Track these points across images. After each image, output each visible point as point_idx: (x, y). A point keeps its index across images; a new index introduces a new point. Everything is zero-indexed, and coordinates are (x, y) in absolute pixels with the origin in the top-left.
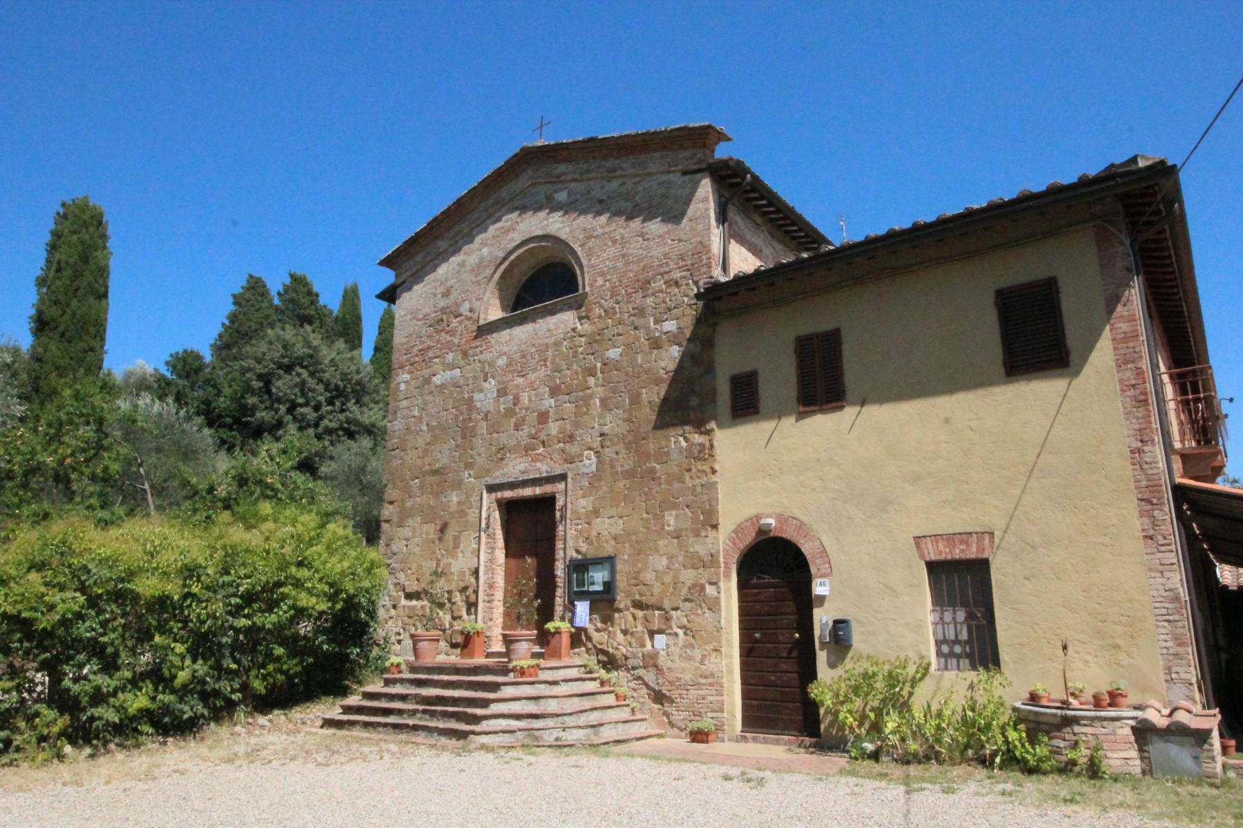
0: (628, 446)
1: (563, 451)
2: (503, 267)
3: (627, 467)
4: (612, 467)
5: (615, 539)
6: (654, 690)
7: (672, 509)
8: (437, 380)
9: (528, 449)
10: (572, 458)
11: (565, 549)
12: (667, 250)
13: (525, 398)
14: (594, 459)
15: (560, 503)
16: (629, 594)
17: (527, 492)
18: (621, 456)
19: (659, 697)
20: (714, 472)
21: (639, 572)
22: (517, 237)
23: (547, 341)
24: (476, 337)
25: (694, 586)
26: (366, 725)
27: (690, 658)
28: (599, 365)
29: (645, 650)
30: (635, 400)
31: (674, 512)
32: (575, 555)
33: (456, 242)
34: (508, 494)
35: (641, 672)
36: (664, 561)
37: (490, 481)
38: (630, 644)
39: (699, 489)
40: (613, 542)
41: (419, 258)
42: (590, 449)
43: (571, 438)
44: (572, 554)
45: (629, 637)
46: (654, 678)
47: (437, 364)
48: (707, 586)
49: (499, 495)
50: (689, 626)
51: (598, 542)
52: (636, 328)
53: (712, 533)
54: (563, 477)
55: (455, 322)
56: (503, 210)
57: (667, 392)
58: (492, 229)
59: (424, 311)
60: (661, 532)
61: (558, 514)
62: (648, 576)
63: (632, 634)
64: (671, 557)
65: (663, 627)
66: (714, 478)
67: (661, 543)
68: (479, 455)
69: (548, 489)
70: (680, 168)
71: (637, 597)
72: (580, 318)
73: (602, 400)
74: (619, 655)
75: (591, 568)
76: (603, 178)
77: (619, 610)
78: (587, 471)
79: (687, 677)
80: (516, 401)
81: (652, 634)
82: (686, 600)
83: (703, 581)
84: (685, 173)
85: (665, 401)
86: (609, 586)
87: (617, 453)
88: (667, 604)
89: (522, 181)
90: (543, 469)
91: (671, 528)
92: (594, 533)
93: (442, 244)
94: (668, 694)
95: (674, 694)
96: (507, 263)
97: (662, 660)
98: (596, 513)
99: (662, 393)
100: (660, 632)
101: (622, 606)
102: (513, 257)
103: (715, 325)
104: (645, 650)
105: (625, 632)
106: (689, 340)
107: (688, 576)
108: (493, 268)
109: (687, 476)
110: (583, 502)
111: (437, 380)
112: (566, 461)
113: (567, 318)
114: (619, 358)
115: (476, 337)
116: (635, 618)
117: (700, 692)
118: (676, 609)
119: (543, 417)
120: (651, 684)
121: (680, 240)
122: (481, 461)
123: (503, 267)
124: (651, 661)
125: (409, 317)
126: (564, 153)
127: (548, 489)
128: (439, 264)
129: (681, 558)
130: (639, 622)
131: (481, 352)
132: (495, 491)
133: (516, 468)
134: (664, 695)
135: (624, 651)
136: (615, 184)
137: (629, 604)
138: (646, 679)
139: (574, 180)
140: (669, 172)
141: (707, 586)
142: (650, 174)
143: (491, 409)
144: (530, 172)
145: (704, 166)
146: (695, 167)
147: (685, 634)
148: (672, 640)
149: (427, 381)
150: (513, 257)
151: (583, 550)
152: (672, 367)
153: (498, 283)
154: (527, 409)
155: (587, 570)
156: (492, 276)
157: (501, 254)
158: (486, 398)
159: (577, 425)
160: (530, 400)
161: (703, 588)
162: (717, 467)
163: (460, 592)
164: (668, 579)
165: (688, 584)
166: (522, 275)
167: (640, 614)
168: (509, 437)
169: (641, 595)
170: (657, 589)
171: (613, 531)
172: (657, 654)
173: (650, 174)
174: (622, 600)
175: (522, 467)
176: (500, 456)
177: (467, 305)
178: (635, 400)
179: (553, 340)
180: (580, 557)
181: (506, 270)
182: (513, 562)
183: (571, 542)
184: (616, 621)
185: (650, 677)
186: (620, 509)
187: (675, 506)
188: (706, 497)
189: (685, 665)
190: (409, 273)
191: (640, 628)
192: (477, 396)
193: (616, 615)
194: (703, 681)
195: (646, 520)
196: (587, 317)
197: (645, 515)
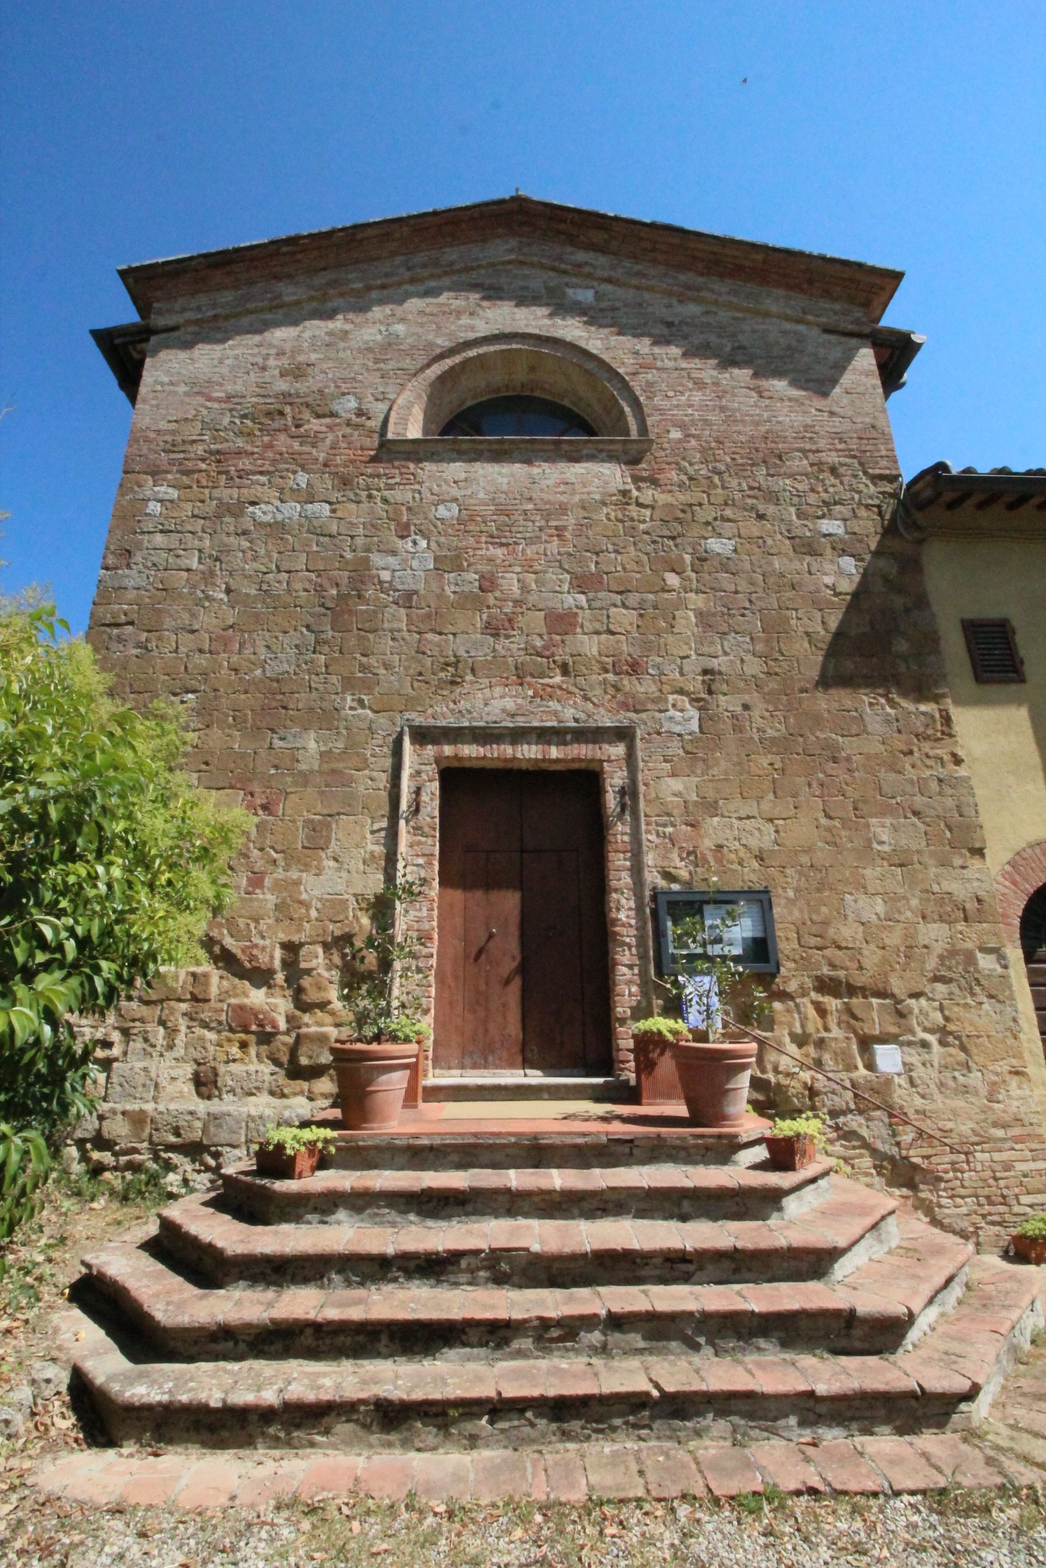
0: (770, 697)
1: (617, 689)
2: (448, 363)
3: (771, 733)
4: (738, 728)
5: (760, 858)
6: (892, 1159)
7: (883, 814)
8: (262, 513)
9: (521, 675)
10: (643, 704)
11: (637, 870)
12: (809, 421)
13: (510, 583)
14: (695, 714)
15: (615, 779)
16: (803, 964)
17: (529, 752)
18: (756, 714)
19: (902, 1174)
20: (958, 761)
21: (826, 923)
22: (483, 329)
23: (564, 498)
24: (374, 459)
25: (953, 953)
26: (392, 1417)
27: (965, 1090)
28: (688, 558)
29: (854, 1075)
30: (775, 628)
31: (888, 821)
32: (661, 883)
33: (325, 298)
34: (470, 751)
35: (854, 1122)
36: (880, 907)
37: (419, 720)
38: (819, 1064)
39: (934, 785)
40: (755, 865)
41: (227, 297)
42: (681, 692)
43: (635, 668)
44: (653, 878)
45: (811, 1049)
46: (885, 1132)
47: (259, 486)
48: (979, 955)
49: (448, 750)
50: (951, 1027)
51: (719, 861)
52: (761, 517)
53: (975, 863)
54: (624, 734)
55: (315, 425)
56: (446, 281)
57: (842, 623)
58: (414, 304)
59: (230, 388)
60: (866, 851)
61: (611, 801)
62: (848, 932)
63: (820, 1043)
64: (892, 899)
65: (893, 1030)
66: (962, 772)
67: (868, 872)
68: (387, 666)
69: (583, 751)
70: (824, 320)
71: (826, 970)
72: (636, 479)
73: (700, 614)
74: (794, 1087)
75: (708, 909)
76: (670, 294)
77: (783, 996)
78: (677, 729)
79: (965, 1128)
80: (488, 584)
81: (866, 1044)
82: (937, 979)
83: (969, 945)
84: (826, 331)
85: (839, 635)
86: (760, 950)
87: (746, 707)
88: (897, 986)
89: (501, 249)
90: (568, 713)
91: (886, 848)
92: (707, 844)
93: (289, 292)
94: (925, 1165)
95: (942, 1162)
96: (458, 359)
97: (902, 1095)
98: (712, 808)
99: (833, 624)
100: (884, 1039)
101: (792, 986)
102: (472, 353)
103: (921, 542)
104: (854, 1075)
105: (801, 1041)
106: (877, 554)
107: (935, 935)
108: (422, 361)
109: (907, 761)
110: (676, 784)
111: (262, 513)
112: (625, 706)
113: (609, 476)
114: (729, 553)
115: (374, 459)
116: (822, 1011)
117: (997, 1156)
118: (916, 995)
119: (562, 623)
120: (879, 1145)
121: (832, 414)
122: (394, 681)
123: (448, 363)
124: (873, 1098)
125: (182, 389)
126: (598, 237)
127: (583, 751)
128: (278, 324)
129: (914, 902)
130: (832, 1021)
131: (390, 487)
132: (435, 742)
133: (493, 703)
134: (916, 1167)
135: (806, 1076)
136: (693, 309)
137: (809, 983)
138: (864, 1132)
139: (609, 280)
140: (799, 321)
141: (979, 955)
142: (767, 314)
143: (421, 587)
144: (513, 243)
145: (867, 330)
146: (851, 327)
147: (942, 1043)
148: (914, 1057)
149: (236, 510)
150: (472, 353)
151: (684, 874)
152: (847, 586)
153: (432, 385)
154: (517, 603)
155: (700, 912)
156: (422, 369)
157: (443, 342)
158: (407, 564)
159: (648, 647)
160: (524, 588)
161: (970, 959)
162: (960, 753)
163: (326, 946)
164: (894, 938)
165: (939, 948)
166: (472, 390)
167: (833, 1004)
168: (468, 640)
169: (833, 966)
170: (871, 957)
171: (754, 843)
172: (888, 1082)
173: (767, 314)
174: (791, 977)
175: (509, 704)
176: (454, 673)
177: (352, 403)
178: (775, 628)
179: (577, 498)
180: (675, 887)
181: (452, 369)
182: (457, 895)
183: (644, 859)
184: (779, 1018)
185: (873, 1128)
186: (765, 806)
187: (885, 811)
188: (950, 802)
189: (959, 1103)
190: (190, 315)
191: (836, 1032)
192: (377, 559)
193: (777, 1005)
194: (1000, 1133)
195: (829, 830)
196: (654, 482)
197: (824, 821)
